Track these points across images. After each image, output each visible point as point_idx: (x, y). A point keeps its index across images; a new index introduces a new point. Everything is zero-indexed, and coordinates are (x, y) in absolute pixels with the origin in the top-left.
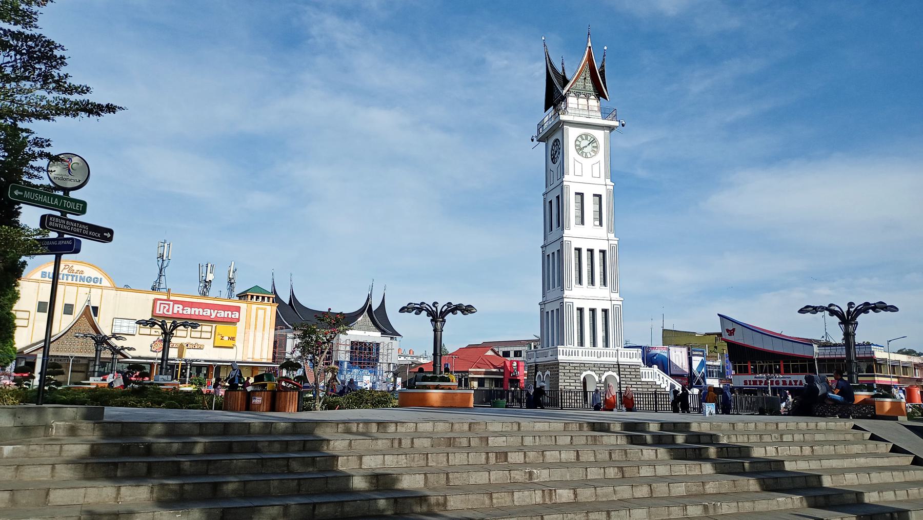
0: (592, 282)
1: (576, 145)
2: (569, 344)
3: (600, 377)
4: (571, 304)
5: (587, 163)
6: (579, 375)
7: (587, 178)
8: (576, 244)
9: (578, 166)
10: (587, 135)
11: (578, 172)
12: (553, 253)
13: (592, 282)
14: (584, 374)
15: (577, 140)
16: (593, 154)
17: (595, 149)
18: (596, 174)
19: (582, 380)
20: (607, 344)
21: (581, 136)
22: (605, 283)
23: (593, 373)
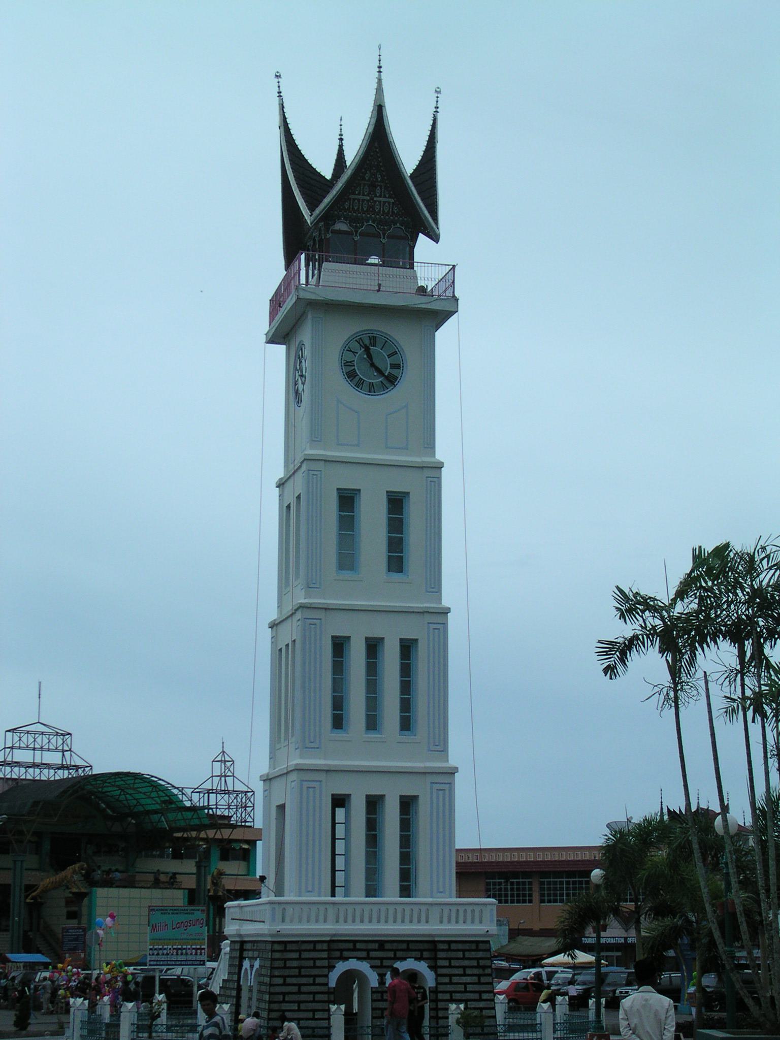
0: (372, 723)
6: (325, 971)
12: (287, 645)
13: (372, 723)
14: (341, 967)
19: (332, 984)
23: (364, 967)
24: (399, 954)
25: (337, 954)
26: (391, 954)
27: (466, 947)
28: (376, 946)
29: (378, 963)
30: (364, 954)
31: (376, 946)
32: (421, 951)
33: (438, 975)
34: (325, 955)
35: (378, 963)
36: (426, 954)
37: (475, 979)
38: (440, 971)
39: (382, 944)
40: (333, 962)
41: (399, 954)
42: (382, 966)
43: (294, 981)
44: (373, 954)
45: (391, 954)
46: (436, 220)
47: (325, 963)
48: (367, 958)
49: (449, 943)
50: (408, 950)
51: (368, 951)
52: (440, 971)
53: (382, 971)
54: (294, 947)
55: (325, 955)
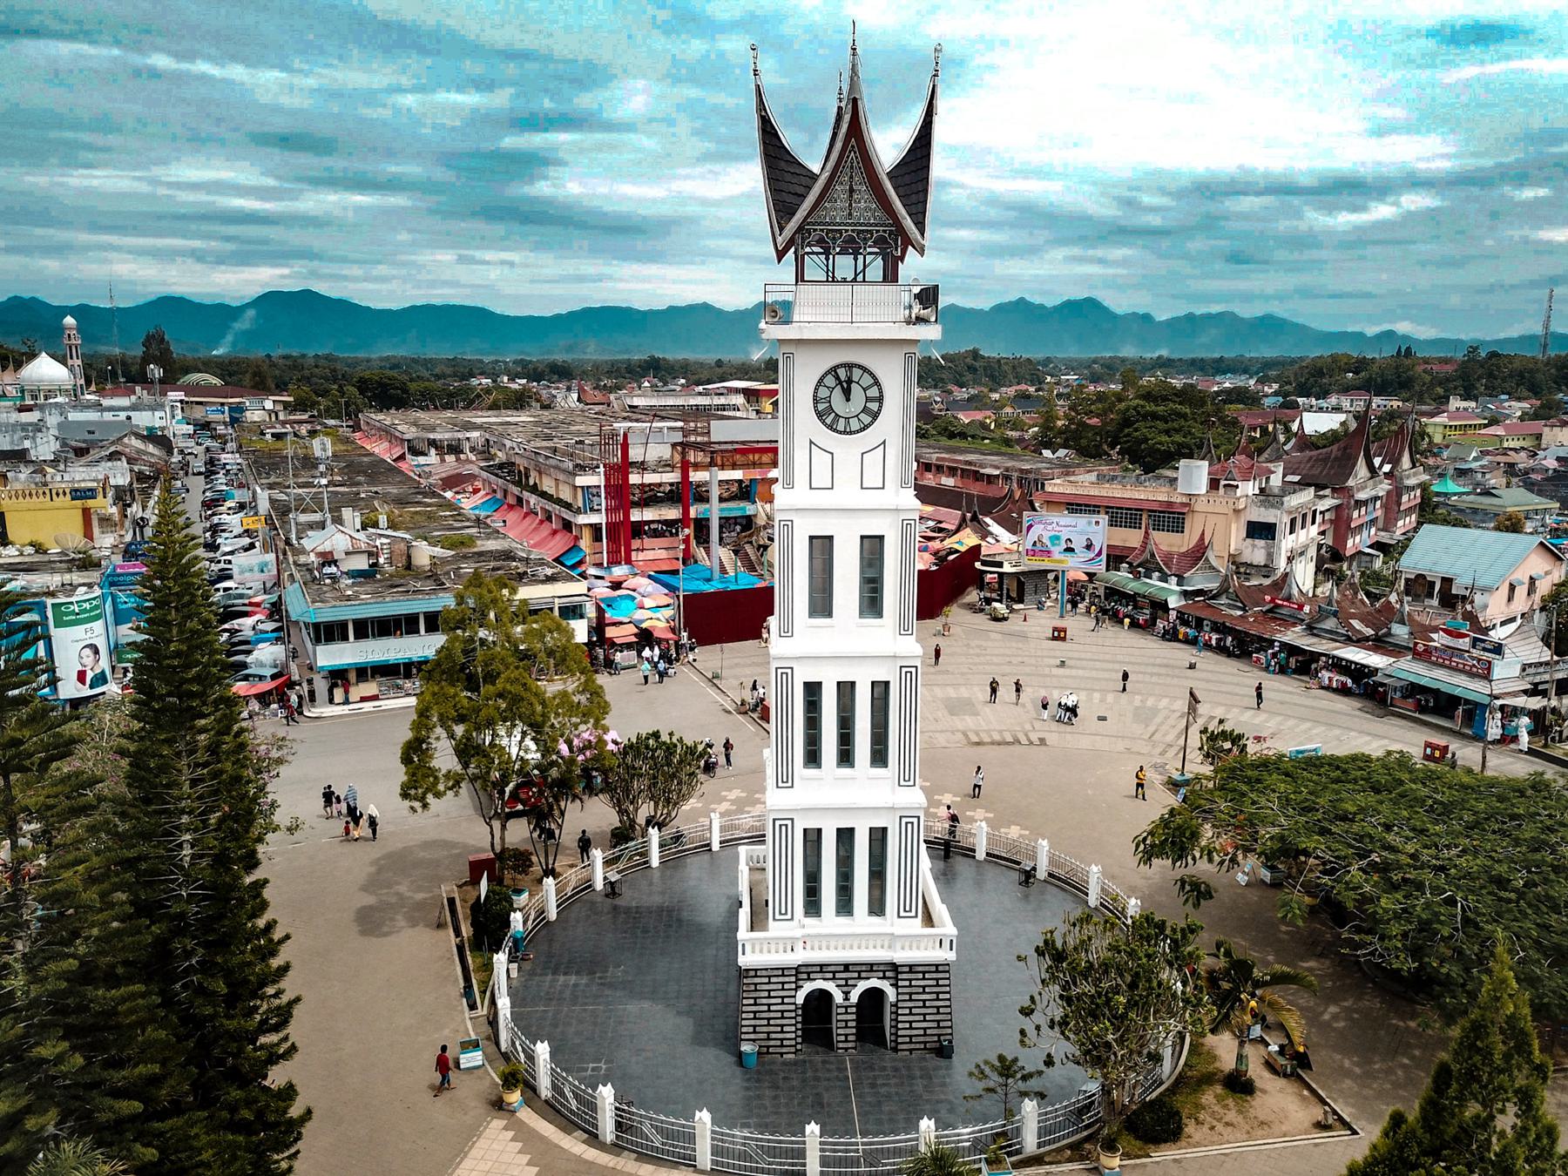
0: (846, 757)
1: (816, 401)
2: (780, 913)
3: (846, 994)
4: (789, 823)
5: (847, 448)
6: (793, 993)
7: (847, 494)
8: (803, 675)
9: (821, 459)
10: (850, 366)
11: (821, 479)
13: (846, 757)
15: (820, 382)
16: (866, 419)
17: (874, 406)
18: (872, 479)
20: (877, 907)
21: (833, 370)
22: (879, 757)
24: (863, 975)
25: (805, 976)
26: (856, 975)
27: (927, 969)
28: (842, 968)
29: (843, 982)
30: (831, 975)
31: (842, 968)
32: (884, 972)
33: (898, 994)
34: (793, 979)
35: (843, 982)
36: (888, 974)
37: (934, 996)
38: (900, 990)
39: (846, 967)
40: (801, 983)
41: (863, 975)
42: (846, 985)
43: (764, 1001)
44: (837, 975)
45: (856, 975)
46: (921, 226)
47: (793, 986)
48: (834, 978)
49: (911, 966)
50: (872, 971)
51: (834, 973)
52: (900, 990)
53: (845, 989)
54: (764, 973)
55: (793, 979)
